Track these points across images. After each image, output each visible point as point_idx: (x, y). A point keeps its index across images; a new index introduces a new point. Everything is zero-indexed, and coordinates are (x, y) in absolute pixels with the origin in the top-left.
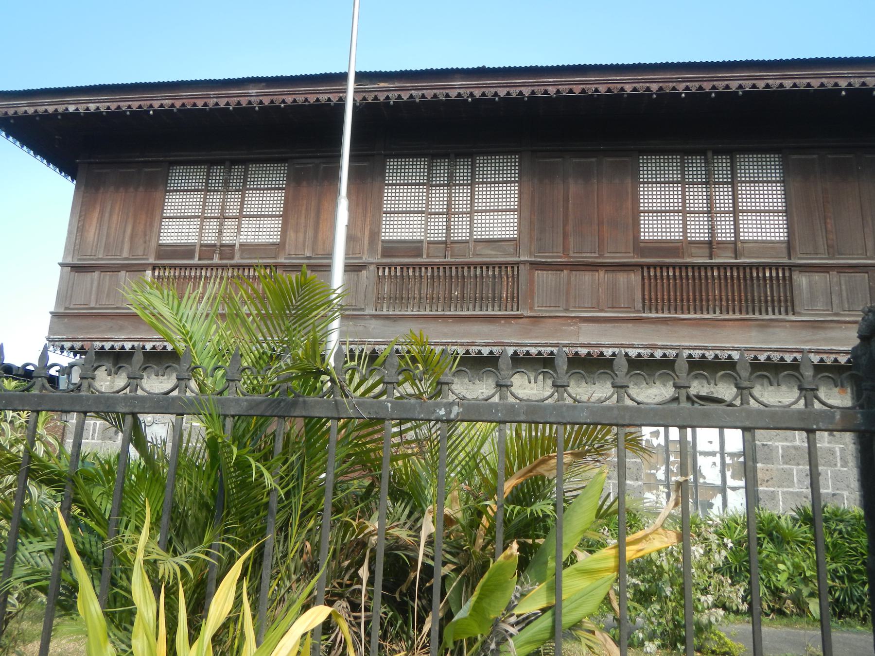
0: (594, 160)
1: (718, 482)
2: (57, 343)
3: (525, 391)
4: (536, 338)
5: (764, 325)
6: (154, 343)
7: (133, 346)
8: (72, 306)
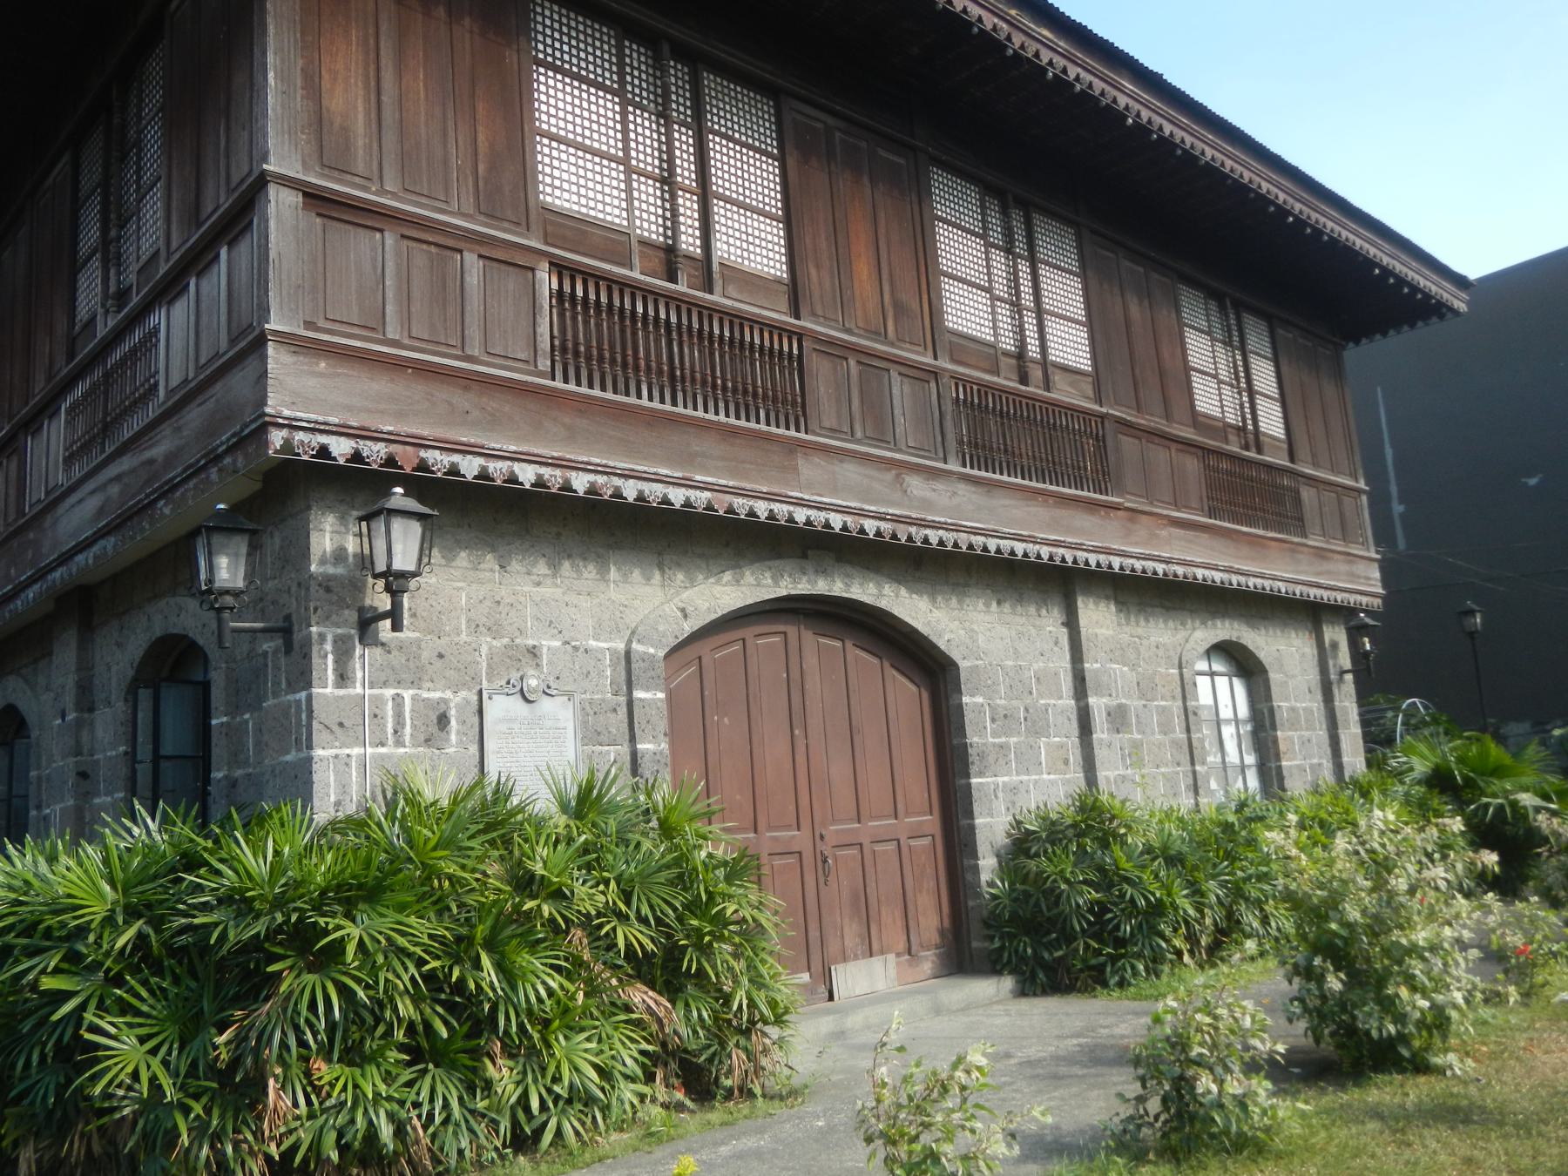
0: (1141, 269)
1: (1237, 761)
2: (300, 436)
3: (1104, 631)
4: (1136, 544)
5: (1294, 549)
6: (591, 477)
7: (539, 476)
8: (321, 323)
